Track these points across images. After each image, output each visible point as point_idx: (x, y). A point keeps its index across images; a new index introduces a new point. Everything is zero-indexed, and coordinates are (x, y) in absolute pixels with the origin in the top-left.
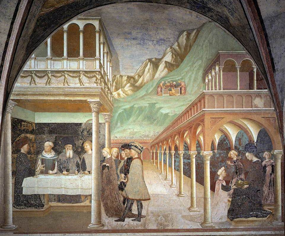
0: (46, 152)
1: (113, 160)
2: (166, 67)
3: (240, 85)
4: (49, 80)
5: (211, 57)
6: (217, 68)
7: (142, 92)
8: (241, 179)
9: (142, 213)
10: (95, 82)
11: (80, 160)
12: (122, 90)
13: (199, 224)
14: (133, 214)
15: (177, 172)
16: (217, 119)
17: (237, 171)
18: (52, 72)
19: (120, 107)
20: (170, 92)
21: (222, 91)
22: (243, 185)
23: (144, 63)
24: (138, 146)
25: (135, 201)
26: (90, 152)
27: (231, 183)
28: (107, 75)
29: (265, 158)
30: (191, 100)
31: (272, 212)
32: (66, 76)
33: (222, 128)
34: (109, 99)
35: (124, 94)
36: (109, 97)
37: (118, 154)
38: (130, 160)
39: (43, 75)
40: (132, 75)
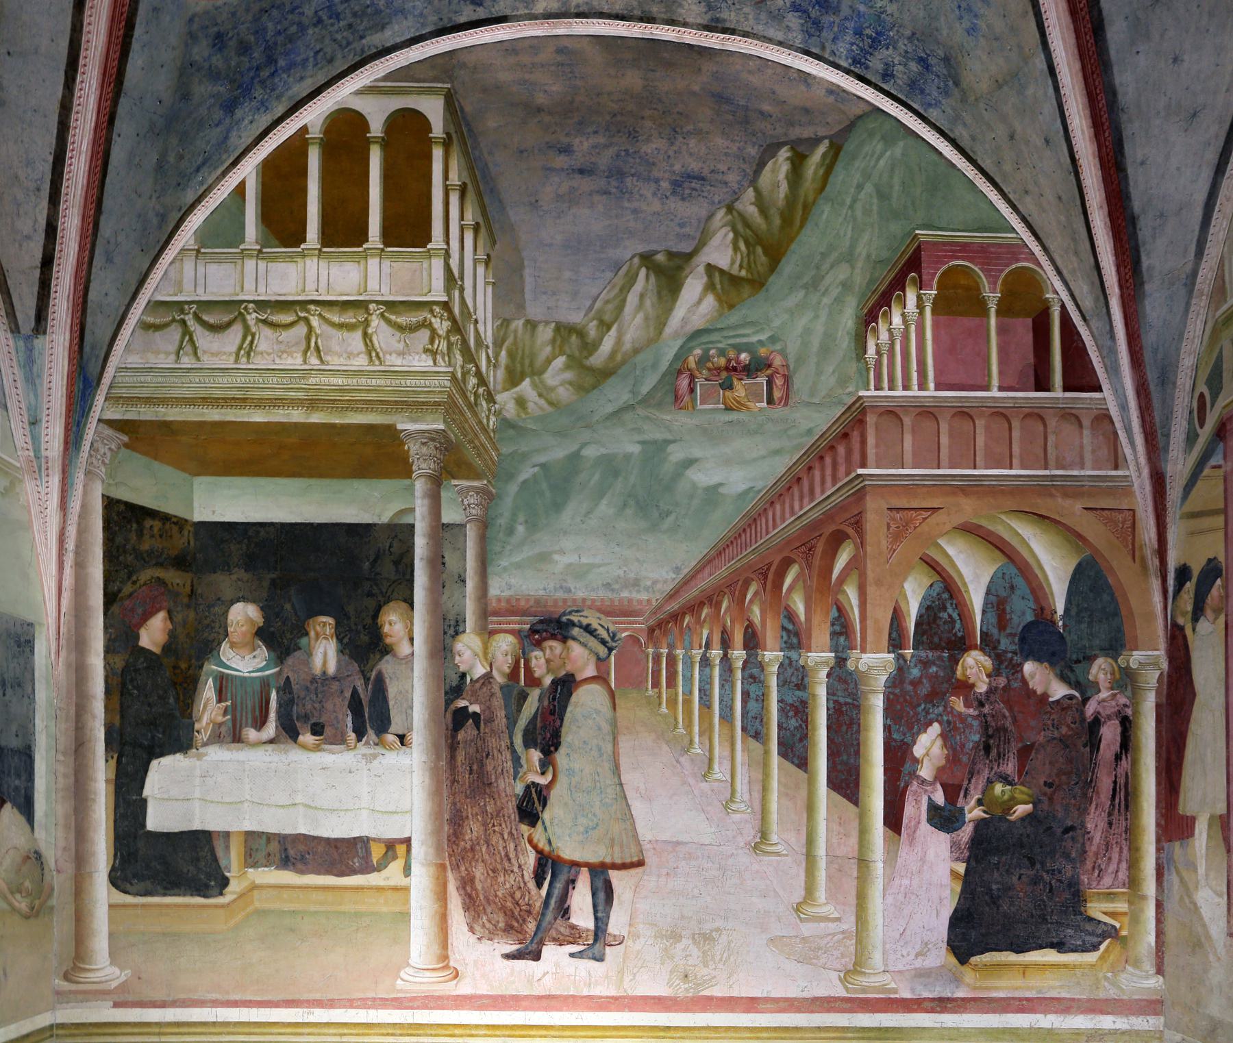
0: (233, 645)
1: (496, 689)
2: (710, 287)
3: (1001, 373)
4: (249, 338)
5: (885, 254)
6: (911, 296)
7: (615, 394)
8: (1006, 780)
9: (610, 926)
10: (426, 351)
11: (366, 684)
12: (534, 385)
13: (834, 976)
14: (573, 927)
15: (753, 743)
16: (914, 514)
17: (992, 741)
18: (261, 305)
19: (525, 456)
20: (728, 393)
21: (931, 392)
22: (1013, 801)
23: (625, 269)
24: (595, 625)
25: (585, 870)
26: (404, 649)
27: (965, 796)
28: (476, 321)
29: (1097, 683)
30: (809, 432)
31: (1118, 925)
32: (315, 322)
33: (933, 553)
34: (480, 422)
35: (542, 402)
36: (483, 415)
37: (517, 663)
38: (565, 686)
39: (226, 318)
40: (576, 318)
